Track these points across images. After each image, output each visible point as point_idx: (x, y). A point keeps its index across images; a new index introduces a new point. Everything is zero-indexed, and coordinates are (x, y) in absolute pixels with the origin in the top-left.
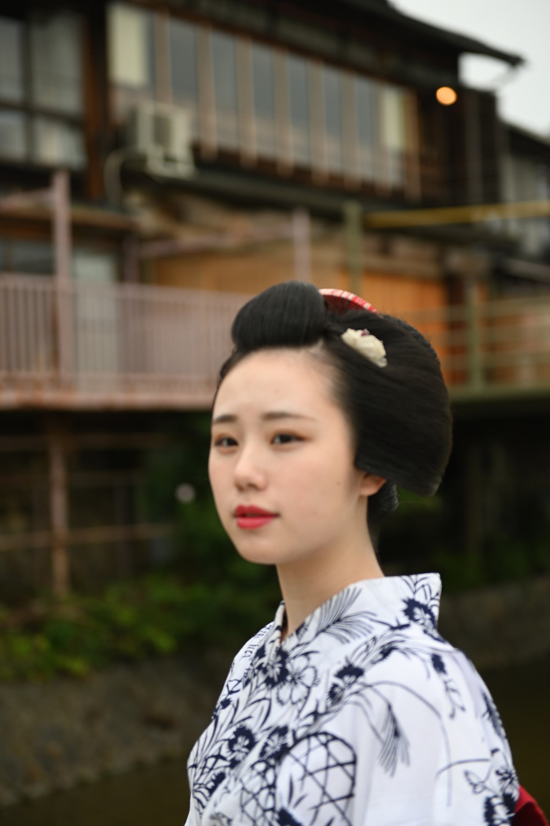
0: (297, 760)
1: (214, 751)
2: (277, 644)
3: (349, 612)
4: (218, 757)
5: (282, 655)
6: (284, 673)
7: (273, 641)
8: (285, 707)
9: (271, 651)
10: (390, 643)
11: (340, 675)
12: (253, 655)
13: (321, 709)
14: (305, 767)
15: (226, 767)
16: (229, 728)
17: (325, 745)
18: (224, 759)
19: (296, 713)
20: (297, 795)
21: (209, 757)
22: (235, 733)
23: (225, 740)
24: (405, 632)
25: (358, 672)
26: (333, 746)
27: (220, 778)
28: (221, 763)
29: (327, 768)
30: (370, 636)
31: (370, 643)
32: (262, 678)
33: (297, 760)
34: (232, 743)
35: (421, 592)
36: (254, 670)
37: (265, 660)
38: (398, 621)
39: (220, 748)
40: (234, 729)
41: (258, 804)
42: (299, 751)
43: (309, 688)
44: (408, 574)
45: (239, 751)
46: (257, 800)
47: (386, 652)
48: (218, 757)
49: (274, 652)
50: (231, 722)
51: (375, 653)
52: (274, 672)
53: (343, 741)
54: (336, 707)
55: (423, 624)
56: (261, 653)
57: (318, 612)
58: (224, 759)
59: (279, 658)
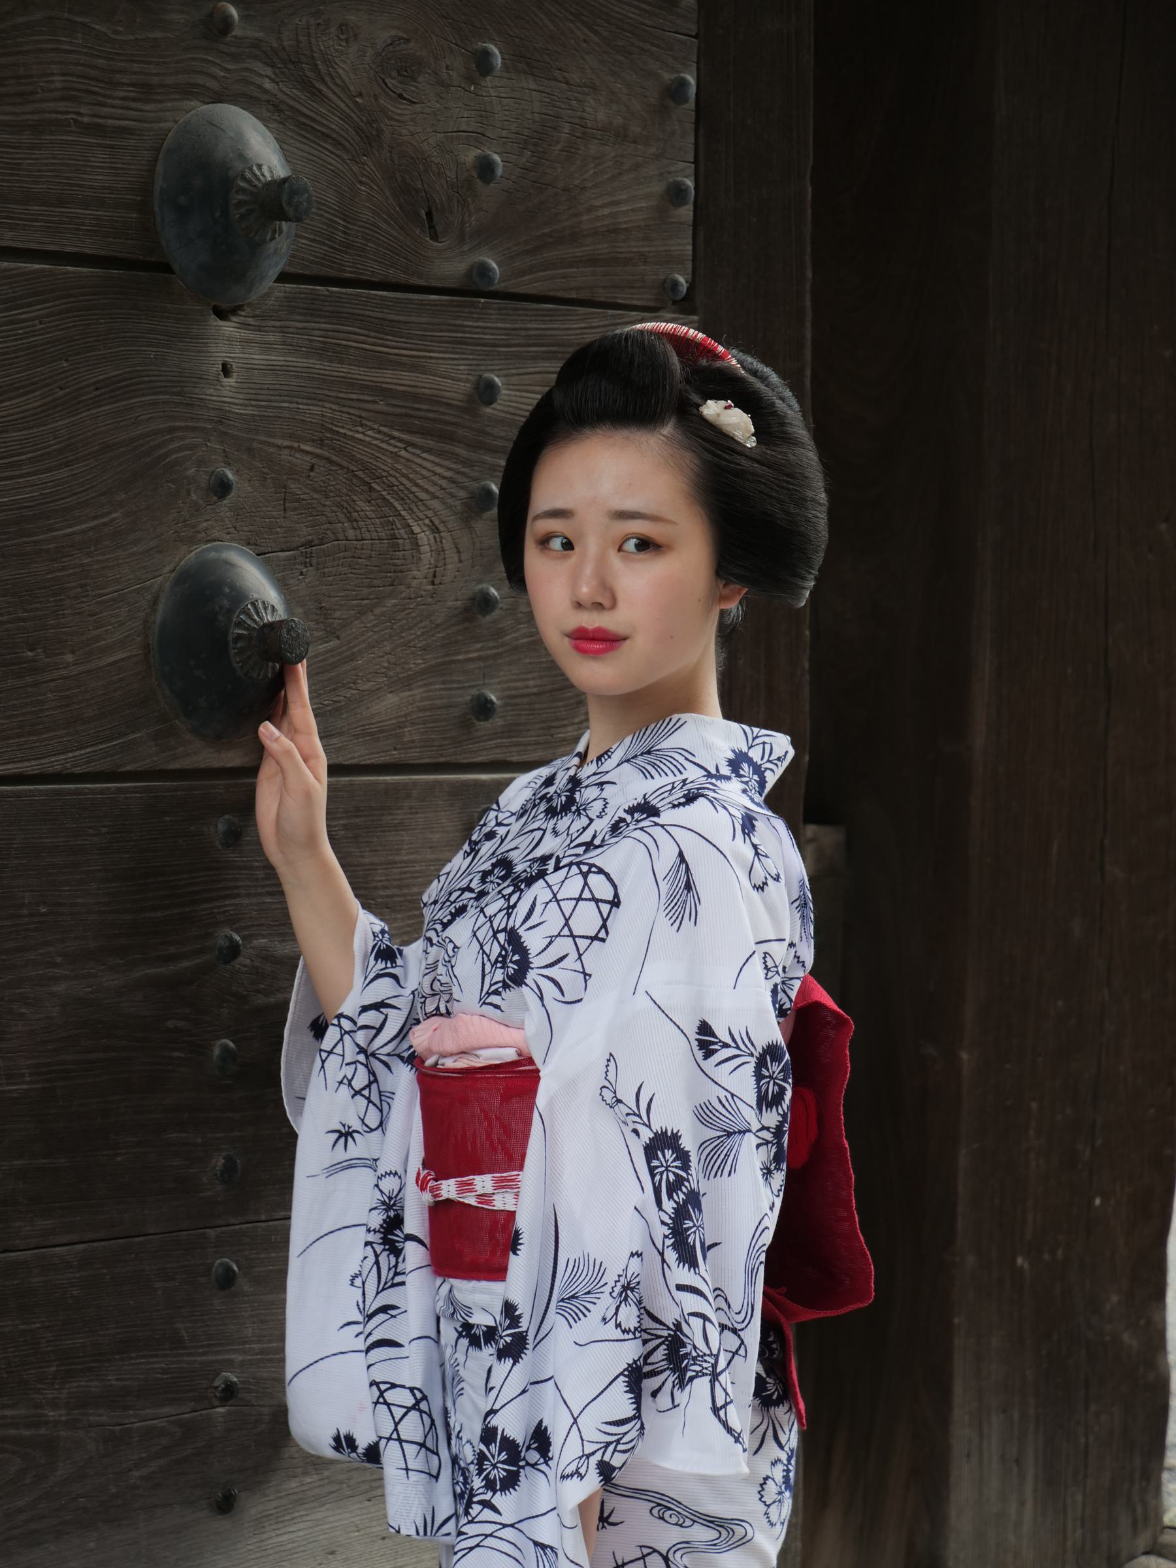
0: (549, 886)
1: (464, 884)
2: (572, 772)
3: (664, 745)
5: (575, 782)
6: (571, 800)
7: (568, 769)
8: (559, 839)
9: (561, 781)
10: (698, 789)
11: (631, 811)
12: (543, 780)
13: (597, 842)
16: (489, 859)
17: (585, 876)
18: (472, 891)
19: (568, 841)
21: (455, 891)
22: (493, 865)
23: (479, 872)
24: (722, 784)
25: (653, 812)
26: (595, 880)
27: (461, 910)
29: (579, 899)
30: (680, 777)
31: (678, 785)
32: (543, 807)
33: (549, 886)
34: (485, 875)
36: (535, 800)
37: (551, 790)
38: (718, 770)
39: (471, 880)
40: (494, 861)
42: (554, 878)
43: (591, 820)
44: (751, 724)
45: (491, 882)
46: (491, 922)
47: (690, 798)
48: (469, 889)
49: (565, 781)
50: (493, 853)
51: (678, 795)
52: (557, 803)
54: (614, 840)
55: (746, 783)
56: (549, 781)
57: (628, 740)
58: (472, 891)
59: (570, 786)
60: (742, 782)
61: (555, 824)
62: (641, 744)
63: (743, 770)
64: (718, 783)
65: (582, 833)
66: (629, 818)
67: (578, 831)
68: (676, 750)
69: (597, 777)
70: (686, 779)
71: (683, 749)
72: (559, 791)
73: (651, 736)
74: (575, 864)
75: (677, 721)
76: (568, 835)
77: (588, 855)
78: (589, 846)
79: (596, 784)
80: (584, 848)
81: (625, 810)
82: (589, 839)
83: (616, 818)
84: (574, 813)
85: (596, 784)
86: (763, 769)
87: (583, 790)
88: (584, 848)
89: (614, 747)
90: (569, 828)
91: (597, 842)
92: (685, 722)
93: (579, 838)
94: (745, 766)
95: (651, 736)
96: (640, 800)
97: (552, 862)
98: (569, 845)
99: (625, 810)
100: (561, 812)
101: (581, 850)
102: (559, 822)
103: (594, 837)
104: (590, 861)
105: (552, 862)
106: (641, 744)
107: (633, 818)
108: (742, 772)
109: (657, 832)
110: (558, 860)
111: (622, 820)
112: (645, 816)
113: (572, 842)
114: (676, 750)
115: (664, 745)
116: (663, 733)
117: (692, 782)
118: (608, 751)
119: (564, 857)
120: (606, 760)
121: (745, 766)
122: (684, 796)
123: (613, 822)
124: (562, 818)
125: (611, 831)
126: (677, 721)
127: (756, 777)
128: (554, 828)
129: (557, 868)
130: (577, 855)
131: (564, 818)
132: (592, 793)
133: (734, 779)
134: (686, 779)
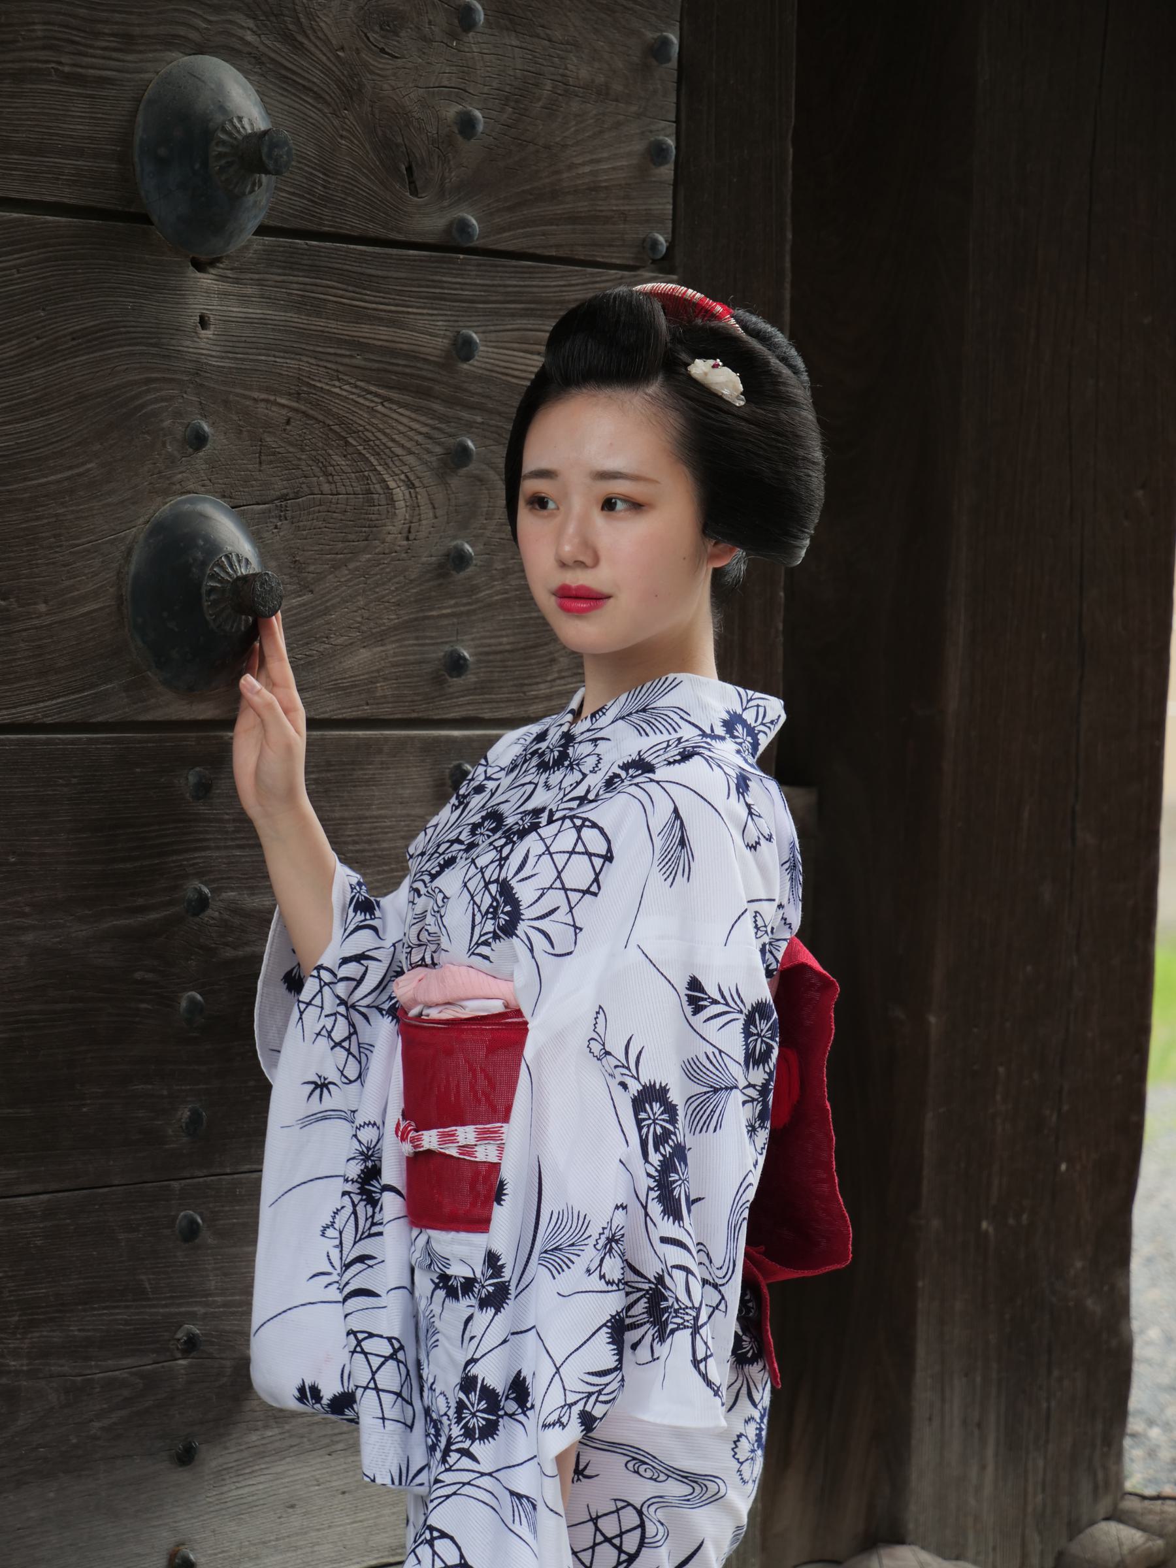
0: (542, 839)
2: (565, 728)
4: (458, 841)
6: (564, 755)
7: (561, 725)
8: (552, 793)
9: (554, 737)
10: (693, 747)
11: (626, 767)
12: (533, 737)
13: (591, 796)
15: (460, 850)
16: (479, 812)
17: (579, 829)
18: (461, 842)
19: (561, 795)
24: (716, 744)
26: (587, 833)
28: (456, 847)
29: (572, 852)
30: (675, 736)
31: (673, 744)
32: (535, 761)
33: (542, 839)
35: (753, 711)
37: (543, 745)
38: (712, 730)
40: (484, 813)
41: (483, 877)
42: (547, 831)
43: (585, 775)
45: (481, 834)
47: (686, 756)
48: (458, 841)
49: (557, 736)
50: (483, 806)
51: (673, 752)
52: (549, 758)
53: (601, 830)
54: (608, 795)
55: (740, 744)
56: (541, 737)
57: (623, 697)
58: (461, 842)
59: (563, 741)
60: (736, 743)
64: (713, 742)
74: (568, 817)
76: (560, 789)
77: (579, 811)
78: (583, 800)
80: (578, 802)
82: (582, 794)
87: (576, 746)
88: (578, 802)
90: (561, 782)
91: (591, 796)
94: (739, 727)
97: (545, 815)
100: (553, 767)
101: (574, 804)
103: (588, 791)
104: (583, 815)
105: (545, 815)
108: (736, 733)
109: (652, 788)
110: (551, 814)
112: (640, 772)
113: (565, 796)
118: (603, 708)
121: (739, 727)
127: (749, 739)
128: (546, 782)
130: (571, 809)
133: (729, 740)
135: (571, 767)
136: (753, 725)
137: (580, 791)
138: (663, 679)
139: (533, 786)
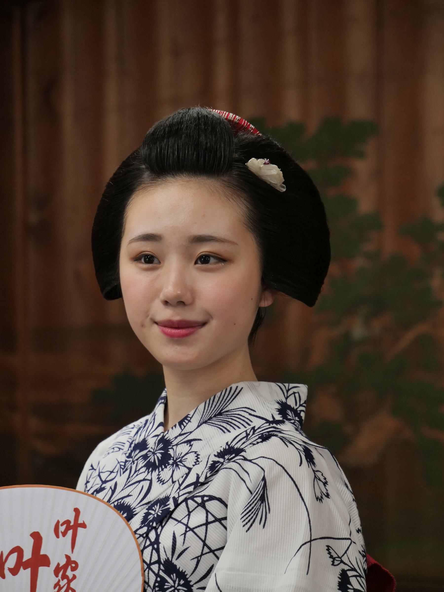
14: (187, 526)
20: (179, 548)
60: (291, 423)
61: (159, 475)
62: (212, 409)
63: (289, 415)
64: (278, 426)
65: (186, 478)
66: (221, 460)
67: (182, 477)
68: (241, 409)
69: (183, 437)
70: (255, 427)
71: (246, 408)
72: (152, 451)
73: (219, 402)
74: (189, 498)
75: (236, 389)
76: (173, 482)
77: (196, 492)
78: (197, 484)
79: (185, 442)
80: (193, 487)
81: (215, 456)
82: (194, 480)
83: (210, 462)
84: (173, 465)
85: (185, 442)
86: (299, 412)
87: (174, 447)
88: (193, 487)
89: (191, 413)
90: (172, 476)
91: (202, 480)
92: (242, 388)
93: (185, 482)
94: (289, 412)
95: (219, 402)
96: (224, 446)
97: (171, 502)
98: (179, 488)
99: (215, 456)
100: (160, 465)
101: (191, 488)
102: (161, 473)
103: (198, 477)
104: (200, 494)
105: (171, 502)
106: (212, 409)
107: (224, 459)
108: (289, 417)
109: (247, 465)
110: (175, 500)
111: (215, 463)
112: (234, 455)
113: (180, 485)
114: (241, 409)
115: (230, 407)
116: (228, 399)
117: (259, 428)
118: (187, 417)
119: (179, 496)
120: (187, 424)
121: (289, 412)
122: (259, 438)
123: (209, 465)
124: (162, 470)
125: (210, 471)
126: (236, 389)
127: (297, 418)
128: (159, 478)
129: (177, 505)
130: (190, 493)
131: (165, 469)
132: (183, 449)
133: (287, 422)
134: (255, 427)
135: (176, 464)
136: (295, 408)
137: (192, 478)
138: (229, 389)
139: (148, 482)
